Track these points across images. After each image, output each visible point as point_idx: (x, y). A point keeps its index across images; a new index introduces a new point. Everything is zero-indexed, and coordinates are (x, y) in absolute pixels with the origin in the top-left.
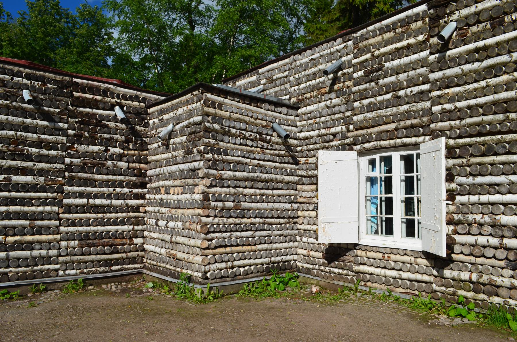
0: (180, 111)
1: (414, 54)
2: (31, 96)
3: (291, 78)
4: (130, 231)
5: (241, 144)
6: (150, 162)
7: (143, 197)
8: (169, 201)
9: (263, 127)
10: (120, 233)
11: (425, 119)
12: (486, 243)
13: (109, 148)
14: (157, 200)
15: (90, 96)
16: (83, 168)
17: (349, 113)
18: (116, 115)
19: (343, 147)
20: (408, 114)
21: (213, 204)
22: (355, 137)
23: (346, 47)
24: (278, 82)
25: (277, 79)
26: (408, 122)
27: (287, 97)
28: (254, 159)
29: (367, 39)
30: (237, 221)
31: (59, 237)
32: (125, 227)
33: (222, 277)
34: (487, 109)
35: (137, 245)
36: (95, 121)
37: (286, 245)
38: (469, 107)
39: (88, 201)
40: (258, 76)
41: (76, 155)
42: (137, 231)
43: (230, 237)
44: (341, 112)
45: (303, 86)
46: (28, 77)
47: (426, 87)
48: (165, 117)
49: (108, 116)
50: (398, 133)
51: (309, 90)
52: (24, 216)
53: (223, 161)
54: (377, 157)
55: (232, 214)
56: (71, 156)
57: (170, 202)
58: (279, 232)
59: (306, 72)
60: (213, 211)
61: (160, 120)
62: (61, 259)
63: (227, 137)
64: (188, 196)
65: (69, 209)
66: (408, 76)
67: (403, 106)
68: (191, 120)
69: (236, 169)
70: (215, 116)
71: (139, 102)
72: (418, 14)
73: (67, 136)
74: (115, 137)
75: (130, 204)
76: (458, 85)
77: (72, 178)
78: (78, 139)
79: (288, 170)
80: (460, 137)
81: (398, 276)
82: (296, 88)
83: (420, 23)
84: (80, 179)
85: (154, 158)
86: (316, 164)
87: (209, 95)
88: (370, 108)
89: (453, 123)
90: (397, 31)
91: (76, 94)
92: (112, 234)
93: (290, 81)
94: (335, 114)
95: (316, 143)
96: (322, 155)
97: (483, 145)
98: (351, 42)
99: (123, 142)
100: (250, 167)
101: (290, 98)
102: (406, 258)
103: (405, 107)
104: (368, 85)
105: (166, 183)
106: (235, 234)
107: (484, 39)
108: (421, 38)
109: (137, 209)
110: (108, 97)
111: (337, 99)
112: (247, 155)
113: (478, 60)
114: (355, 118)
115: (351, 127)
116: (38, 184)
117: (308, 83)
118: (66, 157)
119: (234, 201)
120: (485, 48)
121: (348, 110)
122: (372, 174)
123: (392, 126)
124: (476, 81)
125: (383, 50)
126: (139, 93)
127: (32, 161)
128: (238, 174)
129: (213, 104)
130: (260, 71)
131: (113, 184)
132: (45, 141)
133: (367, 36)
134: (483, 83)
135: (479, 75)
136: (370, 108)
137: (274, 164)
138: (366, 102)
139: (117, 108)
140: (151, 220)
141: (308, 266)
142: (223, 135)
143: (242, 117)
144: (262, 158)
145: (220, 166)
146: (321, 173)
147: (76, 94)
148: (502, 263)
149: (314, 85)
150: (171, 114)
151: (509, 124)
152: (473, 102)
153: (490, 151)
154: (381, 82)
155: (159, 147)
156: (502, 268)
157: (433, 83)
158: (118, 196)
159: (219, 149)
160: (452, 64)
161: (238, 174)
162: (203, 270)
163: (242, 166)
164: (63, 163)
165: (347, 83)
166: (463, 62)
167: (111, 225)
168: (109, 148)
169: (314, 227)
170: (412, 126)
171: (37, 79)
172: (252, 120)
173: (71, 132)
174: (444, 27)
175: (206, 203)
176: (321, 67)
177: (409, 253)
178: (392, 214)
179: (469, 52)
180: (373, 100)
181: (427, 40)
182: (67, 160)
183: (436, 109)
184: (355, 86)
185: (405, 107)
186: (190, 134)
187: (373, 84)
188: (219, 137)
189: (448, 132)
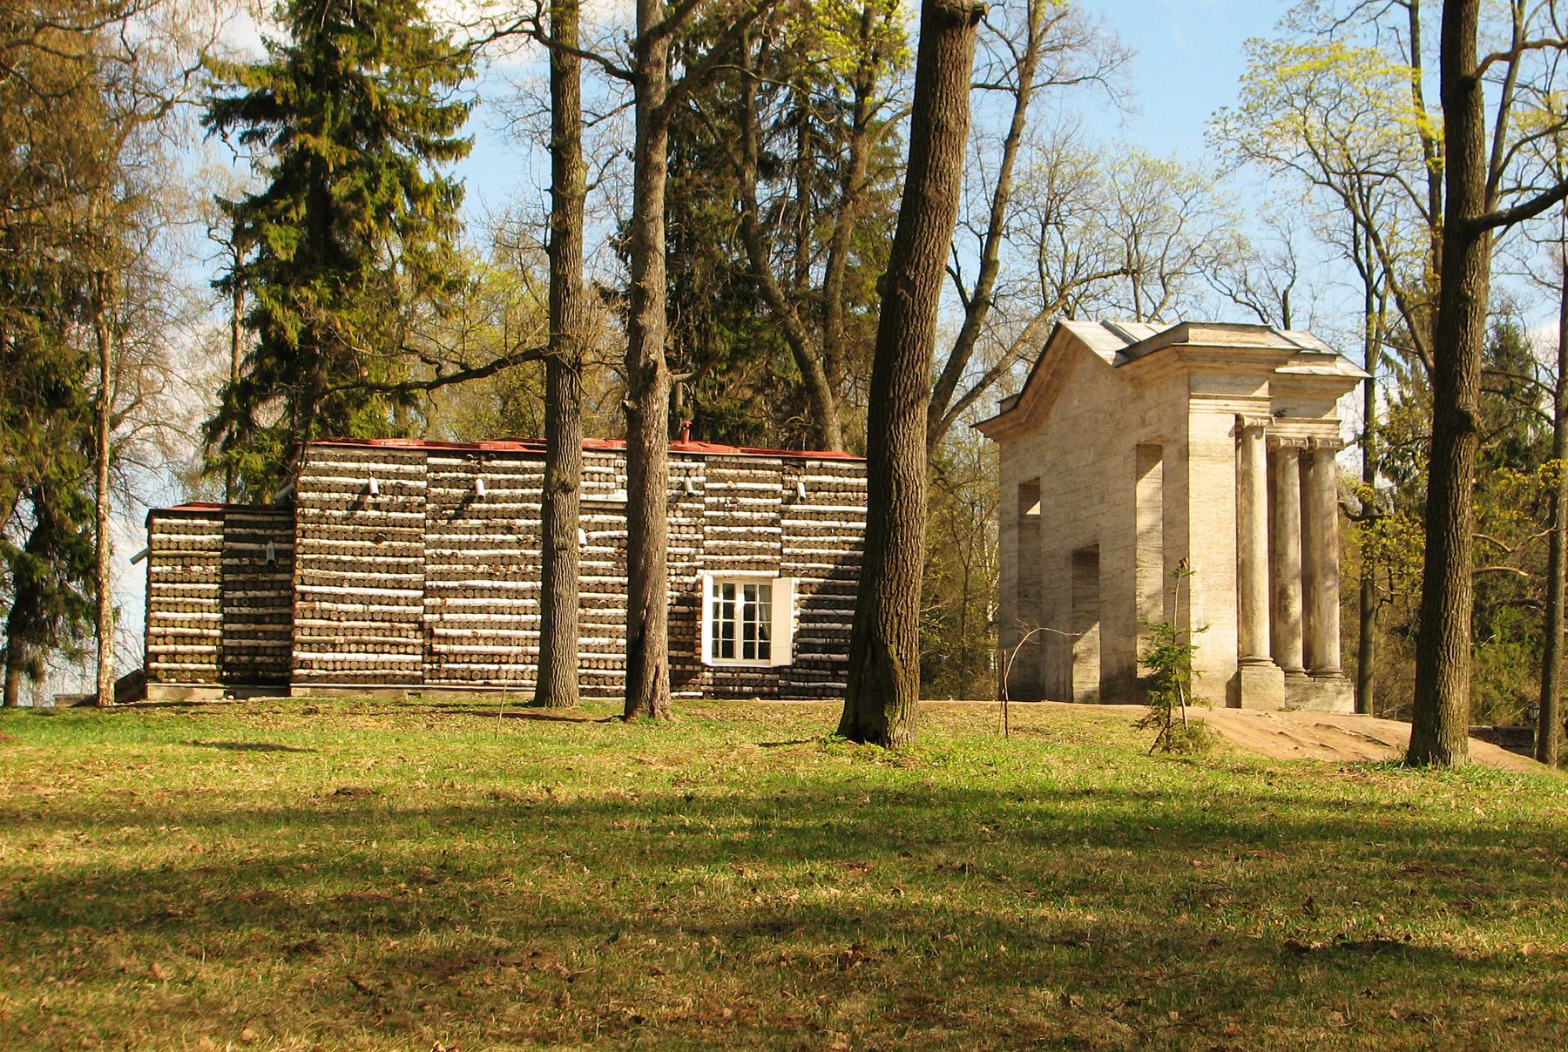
20: (761, 551)
38: (811, 555)
122: (716, 600)
125: (741, 485)
154: (735, 513)
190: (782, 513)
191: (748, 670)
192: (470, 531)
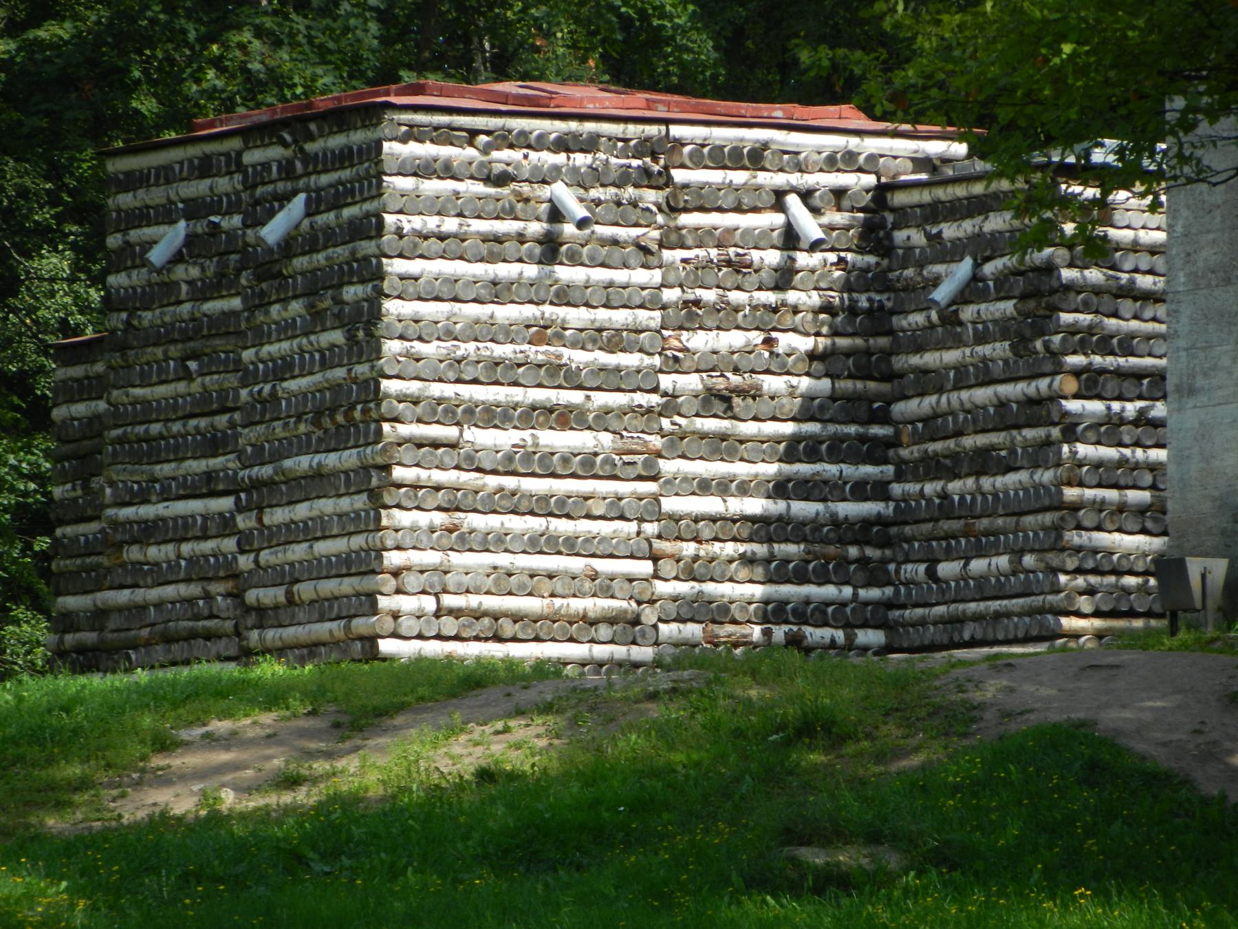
6: (901, 376)
7: (879, 491)
8: (968, 498)
10: (816, 609)
13: (774, 334)
14: (929, 501)
42: (866, 604)
46: (563, 145)
48: (950, 231)
52: (570, 546)
53: (1119, 373)
56: (675, 365)
61: (929, 237)
65: (676, 527)
71: (860, 170)
75: (841, 515)
84: (703, 436)
85: (915, 360)
91: (679, 175)
92: (794, 611)
99: (817, 311)
110: (764, 169)
116: (596, 454)
119: (1153, 487)
127: (580, 387)
132: (607, 325)
139: (793, 201)
140: (910, 567)
142: (1117, 296)
147: (679, 175)
150: (968, 227)
164: (655, 390)
167: (788, 581)
168: (774, 334)
173: (671, 295)
182: (666, 381)
192: (287, 330)
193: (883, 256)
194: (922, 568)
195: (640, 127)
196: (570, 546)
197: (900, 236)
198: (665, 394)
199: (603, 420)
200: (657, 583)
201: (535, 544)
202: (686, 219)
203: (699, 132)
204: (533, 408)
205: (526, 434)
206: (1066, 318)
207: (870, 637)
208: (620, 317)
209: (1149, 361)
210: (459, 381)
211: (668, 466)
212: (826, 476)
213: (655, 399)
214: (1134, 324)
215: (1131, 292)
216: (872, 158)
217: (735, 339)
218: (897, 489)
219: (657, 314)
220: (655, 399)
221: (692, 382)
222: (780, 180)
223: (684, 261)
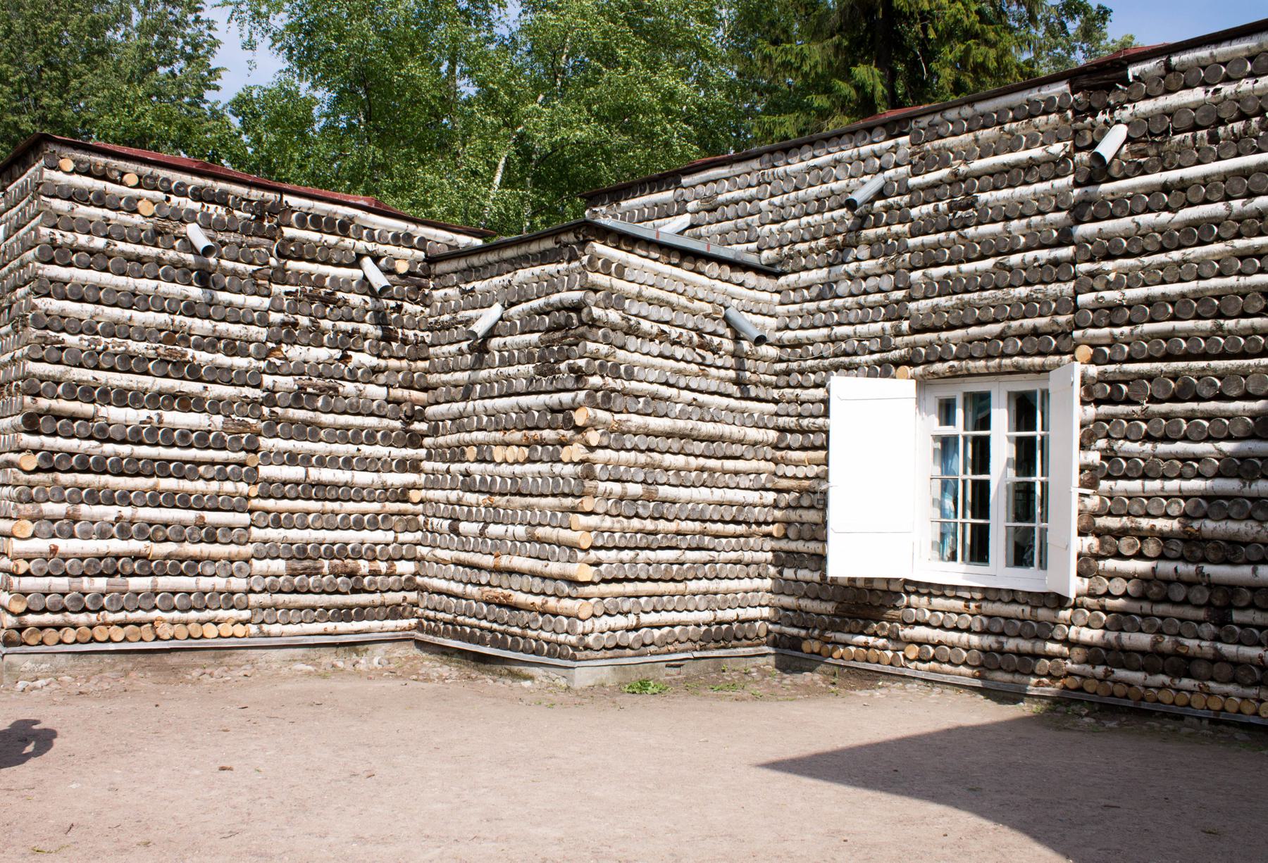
0: (523, 274)
1: (1041, 180)
2: (212, 239)
3: (763, 204)
4: (387, 545)
5: (661, 355)
7: (415, 467)
8: (489, 479)
9: (706, 316)
10: (368, 548)
11: (1062, 319)
12: (1172, 575)
13: (349, 353)
15: (315, 236)
16: (298, 398)
17: (899, 295)
18: (365, 278)
19: (885, 369)
20: (1028, 307)
21: (602, 486)
22: (913, 346)
23: (895, 149)
24: (730, 211)
25: (727, 204)
26: (1028, 323)
27: (753, 246)
28: (688, 388)
29: (941, 137)
30: (649, 525)
31: (249, 549)
32: (379, 536)
33: (618, 646)
34: (1180, 307)
35: (401, 575)
36: (322, 291)
37: (746, 584)
38: (1149, 301)
39: (307, 472)
40: (679, 191)
41: (284, 370)
43: (634, 562)
44: (880, 291)
45: (792, 224)
46: (198, 195)
47: (1067, 252)
49: (348, 281)
50: (1006, 346)
51: (807, 236)
52: (183, 501)
53: (624, 393)
54: (957, 392)
55: (641, 511)
56: (274, 370)
57: (493, 481)
58: (733, 555)
59: (801, 193)
60: (603, 502)
61: (464, 292)
62: (252, 597)
63: (634, 338)
64: (544, 468)
65: (272, 489)
66: (1029, 226)
67: (1018, 290)
68: (555, 298)
69: (650, 411)
70: (610, 291)
72: (1051, 99)
73: (269, 325)
74: (364, 328)
75: (389, 483)
76: (1127, 255)
77: (275, 420)
78: (289, 332)
79: (756, 416)
80: (1131, 359)
81: (995, 646)
82: (775, 227)
83: (1054, 117)
84: (292, 422)
86: (826, 402)
87: (598, 247)
88: (946, 287)
89: (1117, 331)
90: (1007, 127)
92: (353, 550)
93: (760, 211)
94: (866, 293)
95: (822, 357)
96: (838, 382)
97: (1175, 380)
98: (907, 138)
100: (679, 406)
101: (760, 250)
102: (1014, 610)
103: (1023, 291)
104: (942, 236)
105: (480, 436)
106: (644, 555)
107: (1180, 167)
108: (1057, 148)
109: (402, 495)
110: (348, 236)
111: (873, 262)
112: (672, 381)
113: (1167, 208)
114: (912, 306)
115: (905, 325)
116: (210, 432)
117: (804, 220)
118: (264, 372)
119: (644, 482)
120: (1183, 186)
121: (897, 288)
122: (947, 430)
123: (995, 328)
124: (1163, 250)
125: (977, 164)
126: (412, 227)
127: (199, 380)
128: (655, 423)
129: (606, 268)
130: (685, 181)
131: (354, 435)
132: (225, 335)
133: (942, 130)
134: (1176, 255)
135: (1169, 240)
136: (946, 287)
137: (725, 401)
138: (937, 272)
139: (367, 261)
140: (435, 521)
141: (794, 631)
142: (626, 334)
143: (663, 295)
144: (703, 387)
145: (618, 402)
146: (834, 423)
147: (288, 232)
148: (1201, 614)
149: (820, 225)
151: (1222, 341)
152: (1157, 290)
153: (1185, 392)
154: (970, 231)
155: (461, 353)
156: (1199, 622)
157: (1080, 244)
158: (367, 464)
159: (616, 366)
160: (1118, 211)
161: (655, 423)
162: (580, 630)
163: (663, 404)
164: (258, 386)
165: (896, 228)
166: (1140, 209)
168: (349, 353)
169: (813, 547)
170: (1035, 332)
171: (221, 200)
172: (683, 301)
173: (275, 317)
174: (1102, 134)
175: (588, 483)
176: (833, 185)
177: (1020, 598)
178: (986, 516)
179: (1151, 191)
180: (952, 269)
181: (1069, 155)
182: (268, 380)
183: (1085, 299)
184: (913, 236)
185: (1023, 291)
186: (548, 331)
187: (953, 234)
188: (618, 337)
189: (1107, 350)
190: (1079, 213)
191: (1013, 596)
193: (426, 306)
194: (446, 523)
195: (261, 193)
196: (183, 501)
197: (438, 294)
198: (267, 390)
199: (217, 406)
200: (253, 529)
201: (155, 500)
202: (291, 264)
203: (305, 203)
204: (160, 394)
205: (153, 413)
206: (591, 346)
207: (405, 567)
208: (236, 330)
209: (645, 386)
210: (97, 368)
211: (265, 443)
212: (379, 455)
213: (258, 393)
214: (636, 356)
215: (633, 331)
216: (423, 240)
217: (323, 353)
218: (427, 465)
219: (264, 330)
220: (258, 393)
221: (287, 383)
222: (362, 245)
223: (287, 293)
